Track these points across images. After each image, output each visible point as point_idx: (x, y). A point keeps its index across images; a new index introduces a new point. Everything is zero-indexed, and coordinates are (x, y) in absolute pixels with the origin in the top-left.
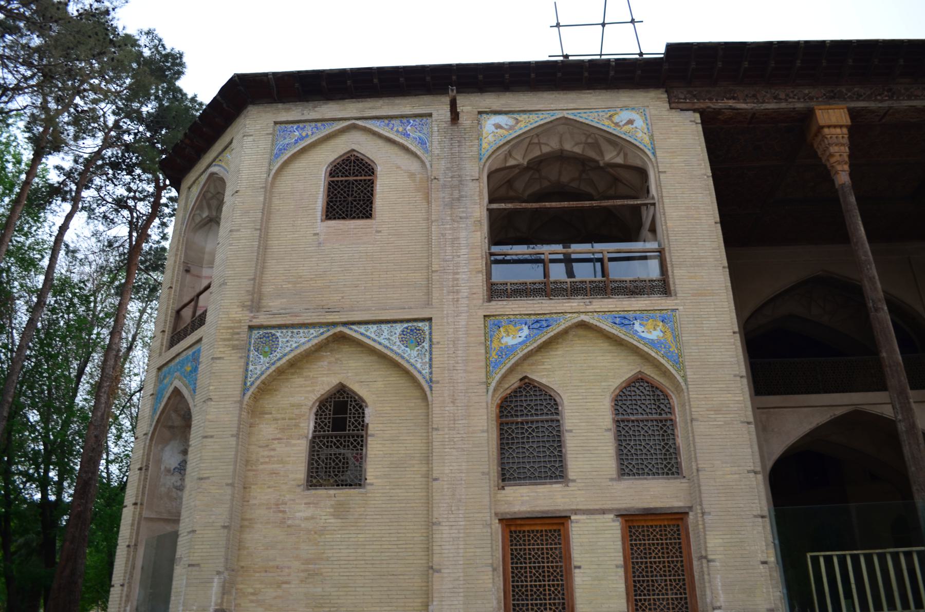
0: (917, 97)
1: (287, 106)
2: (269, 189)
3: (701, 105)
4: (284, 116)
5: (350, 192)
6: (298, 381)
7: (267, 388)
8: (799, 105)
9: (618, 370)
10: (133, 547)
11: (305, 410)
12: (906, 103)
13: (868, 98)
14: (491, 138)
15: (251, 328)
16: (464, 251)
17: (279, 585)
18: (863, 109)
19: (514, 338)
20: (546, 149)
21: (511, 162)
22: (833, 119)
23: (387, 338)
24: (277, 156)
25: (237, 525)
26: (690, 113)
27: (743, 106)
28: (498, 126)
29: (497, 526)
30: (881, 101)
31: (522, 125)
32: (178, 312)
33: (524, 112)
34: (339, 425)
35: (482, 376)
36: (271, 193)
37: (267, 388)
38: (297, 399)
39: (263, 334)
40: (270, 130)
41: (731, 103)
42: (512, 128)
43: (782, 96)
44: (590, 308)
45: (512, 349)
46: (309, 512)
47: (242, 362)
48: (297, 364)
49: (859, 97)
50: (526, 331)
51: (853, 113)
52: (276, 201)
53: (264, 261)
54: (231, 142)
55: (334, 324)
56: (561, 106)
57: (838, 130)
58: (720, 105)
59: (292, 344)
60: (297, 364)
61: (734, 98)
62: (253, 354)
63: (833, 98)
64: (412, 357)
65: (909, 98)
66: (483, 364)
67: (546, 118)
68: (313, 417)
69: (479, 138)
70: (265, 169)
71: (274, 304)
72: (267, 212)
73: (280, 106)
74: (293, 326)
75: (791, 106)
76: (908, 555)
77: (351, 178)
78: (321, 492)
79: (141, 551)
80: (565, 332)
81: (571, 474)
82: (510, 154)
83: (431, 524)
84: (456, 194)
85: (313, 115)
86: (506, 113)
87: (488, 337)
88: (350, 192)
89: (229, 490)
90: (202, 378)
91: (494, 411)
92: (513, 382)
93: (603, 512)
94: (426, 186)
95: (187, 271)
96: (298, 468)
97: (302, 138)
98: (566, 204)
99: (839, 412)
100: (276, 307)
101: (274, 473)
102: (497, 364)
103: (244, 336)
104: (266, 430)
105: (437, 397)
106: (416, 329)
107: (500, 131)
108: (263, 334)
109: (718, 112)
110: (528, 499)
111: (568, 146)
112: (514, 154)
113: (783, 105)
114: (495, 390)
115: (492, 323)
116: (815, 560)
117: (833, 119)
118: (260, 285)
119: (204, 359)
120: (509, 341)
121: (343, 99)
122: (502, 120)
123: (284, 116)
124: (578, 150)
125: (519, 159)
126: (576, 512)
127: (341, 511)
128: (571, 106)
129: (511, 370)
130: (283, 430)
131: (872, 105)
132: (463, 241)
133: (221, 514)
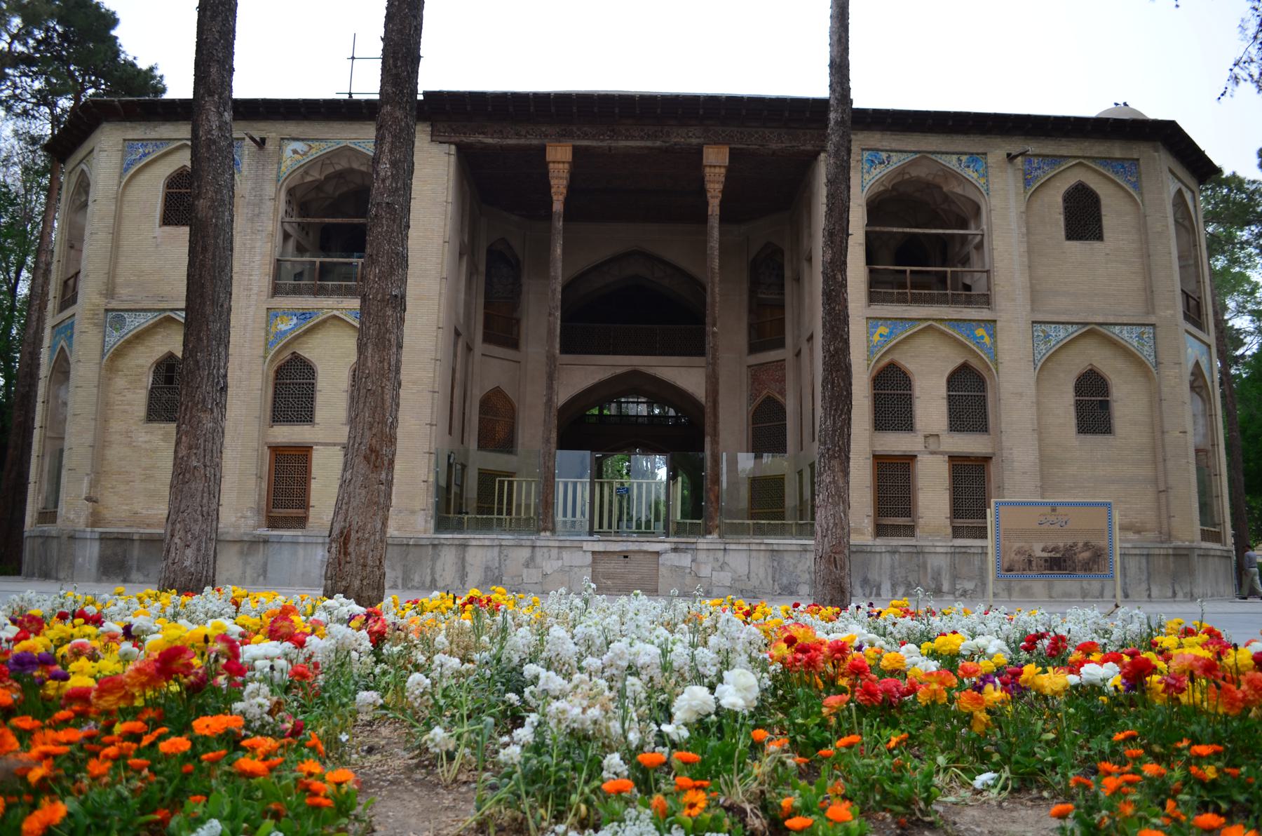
0: (633, 138)
1: (133, 125)
2: (120, 199)
3: (457, 139)
4: (131, 135)
6: (141, 348)
7: (119, 353)
8: (535, 142)
10: (41, 457)
11: (146, 369)
12: (622, 143)
13: (593, 137)
14: (289, 162)
15: (107, 310)
16: (258, 258)
17: (128, 482)
18: (587, 148)
19: (285, 325)
20: (338, 168)
21: (309, 179)
22: (559, 156)
24: (126, 170)
25: (100, 446)
26: (446, 146)
27: (489, 141)
28: (295, 152)
29: (267, 452)
30: (602, 140)
31: (313, 151)
32: (66, 282)
33: (317, 140)
34: (169, 380)
35: (261, 352)
36: (122, 201)
37: (119, 353)
38: (141, 362)
39: (115, 316)
40: (120, 147)
41: (481, 138)
42: (305, 154)
43: (523, 133)
44: (340, 306)
45: (285, 332)
46: (147, 438)
47: (101, 335)
48: (140, 337)
49: (585, 136)
50: (295, 321)
51: (576, 150)
52: (125, 208)
53: (117, 258)
54: (92, 151)
55: (165, 310)
56: (345, 136)
57: (561, 166)
58: (472, 139)
59: (135, 323)
60: (140, 337)
61: (483, 133)
62: (108, 329)
63: (562, 136)
65: (627, 139)
66: (262, 343)
67: (333, 146)
68: (151, 374)
69: (279, 163)
70: (116, 182)
71: (123, 292)
72: (118, 218)
73: (128, 124)
74: (136, 310)
75: (528, 142)
76: (575, 485)
77: (183, 191)
78: (156, 425)
79: (47, 460)
80: (324, 321)
81: (317, 420)
82: (306, 173)
84: (256, 212)
85: (153, 135)
86: (303, 140)
87: (269, 323)
89: (93, 423)
90: (75, 346)
91: (272, 374)
92: (286, 355)
93: (335, 445)
95: (72, 247)
96: (141, 409)
97: (145, 155)
98: (339, 220)
99: (619, 371)
100: (126, 295)
101: (125, 411)
102: (272, 344)
103: (101, 316)
104: (120, 382)
107: (296, 156)
108: (115, 316)
109: (470, 146)
110: (288, 434)
111: (355, 166)
112: (311, 172)
113: (522, 141)
114: (272, 361)
115: (272, 314)
116: (501, 483)
117: (559, 156)
118: (114, 277)
119: (76, 331)
120: (283, 327)
121: (177, 120)
122: (299, 146)
123: (131, 135)
124: (363, 168)
125: (315, 175)
126: (317, 444)
128: (354, 136)
129: (285, 347)
130: (131, 383)
131: (594, 143)
132: (258, 250)
133: (88, 438)
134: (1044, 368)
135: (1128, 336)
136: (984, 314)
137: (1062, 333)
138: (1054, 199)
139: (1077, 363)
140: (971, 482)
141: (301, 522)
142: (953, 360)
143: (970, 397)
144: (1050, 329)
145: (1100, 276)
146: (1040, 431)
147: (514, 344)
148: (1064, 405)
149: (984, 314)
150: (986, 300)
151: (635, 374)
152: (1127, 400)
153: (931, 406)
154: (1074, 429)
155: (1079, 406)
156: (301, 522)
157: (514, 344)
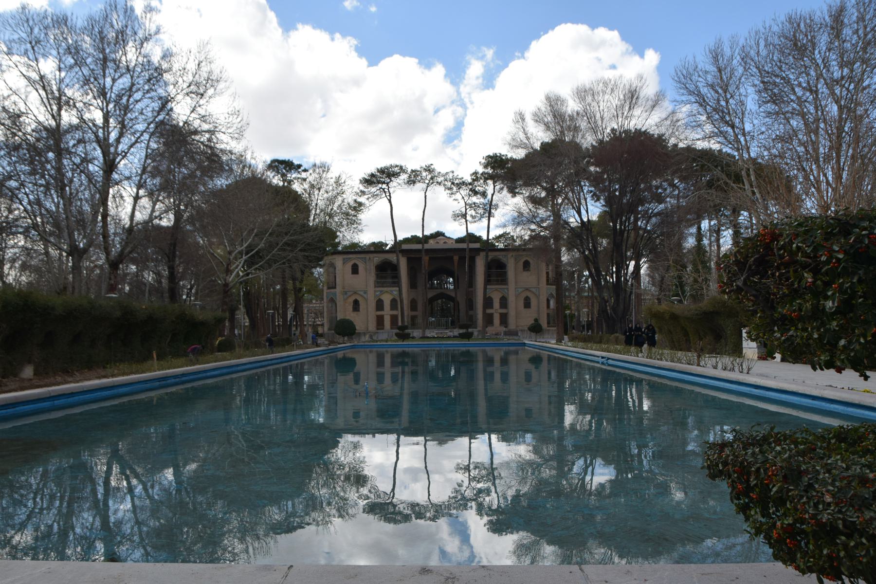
5: (355, 270)
9: (391, 297)
23: (361, 293)
39: (346, 293)
59: (349, 294)
88: (355, 270)
94: (366, 269)
106: (365, 292)
110: (379, 313)
115: (375, 291)
134: (517, 296)
135: (533, 290)
138: (521, 264)
139: (524, 295)
140: (504, 319)
141: (383, 329)
142: (500, 295)
143: (504, 303)
145: (529, 279)
148: (521, 303)
150: (506, 284)
152: (534, 302)
153: (496, 304)
156: (383, 329)
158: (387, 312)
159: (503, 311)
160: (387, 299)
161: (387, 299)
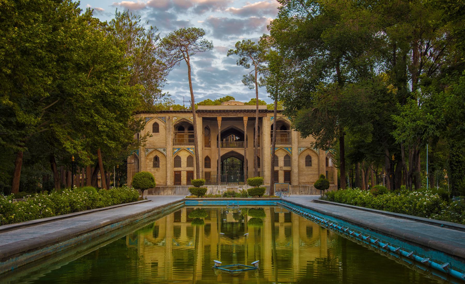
23: (161, 150)
34: (156, 160)
37: (148, 156)
59: (150, 150)
64: (164, 152)
83: (166, 172)
96: (152, 166)
105: (168, 157)
110: (176, 169)
115: (174, 149)
127: (157, 170)
134: (300, 155)
136: (290, 146)
137: (303, 149)
139: (306, 154)
143: (288, 160)
144: (301, 148)
146: (299, 166)
147: (210, 147)
148: (303, 162)
149: (290, 146)
150: (291, 143)
151: (232, 152)
153: (281, 162)
154: (305, 166)
155: (306, 161)
157: (210, 147)
158: (184, 168)
159: (287, 168)
160: (184, 156)
161: (184, 156)
